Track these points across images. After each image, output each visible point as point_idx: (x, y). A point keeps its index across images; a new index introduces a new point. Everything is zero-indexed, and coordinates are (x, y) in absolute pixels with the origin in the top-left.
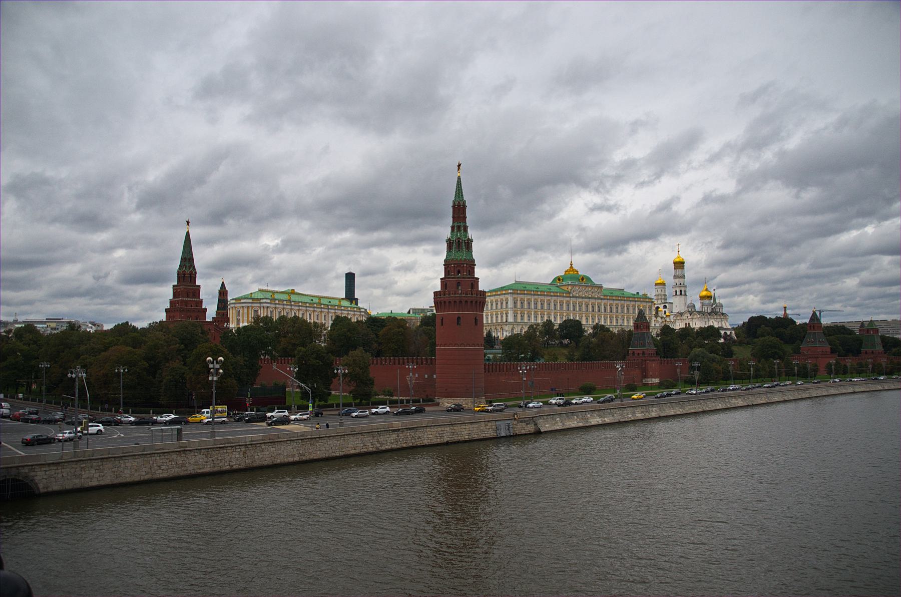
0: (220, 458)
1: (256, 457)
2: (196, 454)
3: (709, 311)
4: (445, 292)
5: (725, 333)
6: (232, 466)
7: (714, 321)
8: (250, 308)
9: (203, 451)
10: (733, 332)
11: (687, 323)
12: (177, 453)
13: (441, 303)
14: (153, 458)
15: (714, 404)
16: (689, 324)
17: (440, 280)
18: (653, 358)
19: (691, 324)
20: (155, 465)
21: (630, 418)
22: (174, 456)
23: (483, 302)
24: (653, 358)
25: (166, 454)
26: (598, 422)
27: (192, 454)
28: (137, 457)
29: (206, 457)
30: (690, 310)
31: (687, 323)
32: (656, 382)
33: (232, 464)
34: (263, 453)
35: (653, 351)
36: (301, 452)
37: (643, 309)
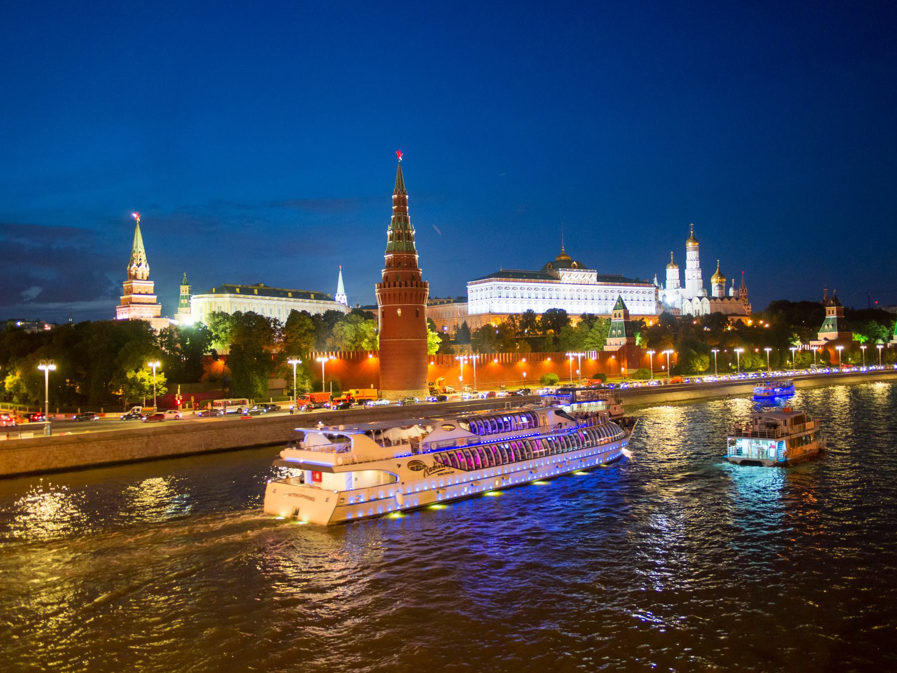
0: (121, 449)
1: (160, 447)
2: (96, 445)
4: (384, 284)
5: (740, 320)
6: (134, 456)
8: (213, 304)
9: (102, 442)
12: (76, 444)
13: (381, 295)
14: (49, 450)
20: (51, 455)
22: (72, 447)
25: (62, 446)
27: (91, 445)
28: (32, 448)
29: (106, 447)
30: (701, 296)
33: (134, 454)
34: (166, 444)
36: (208, 442)
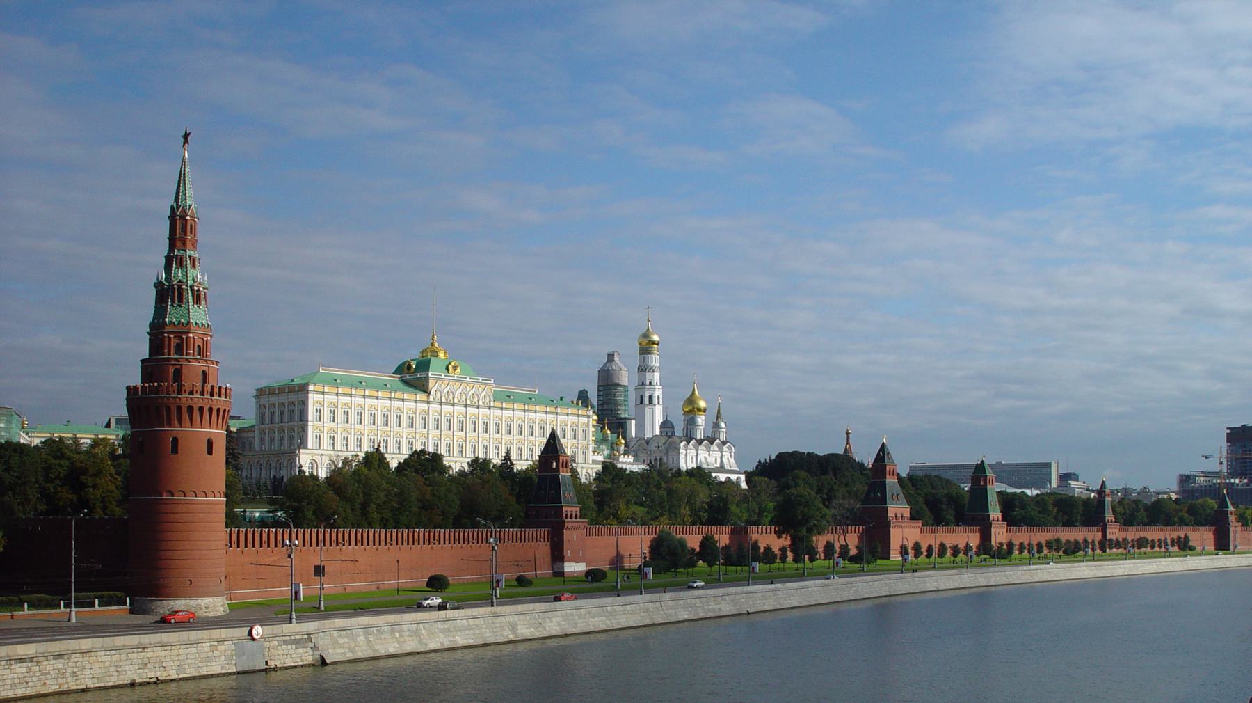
3: (698, 437)
7: (707, 456)
10: (743, 477)
11: (658, 458)
15: (673, 611)
16: (661, 459)
17: (140, 363)
18: (576, 525)
19: (665, 460)
21: (507, 636)
23: (225, 410)
24: (576, 525)
26: (442, 643)
31: (658, 458)
32: (580, 569)
35: (574, 509)
37: (559, 433)
